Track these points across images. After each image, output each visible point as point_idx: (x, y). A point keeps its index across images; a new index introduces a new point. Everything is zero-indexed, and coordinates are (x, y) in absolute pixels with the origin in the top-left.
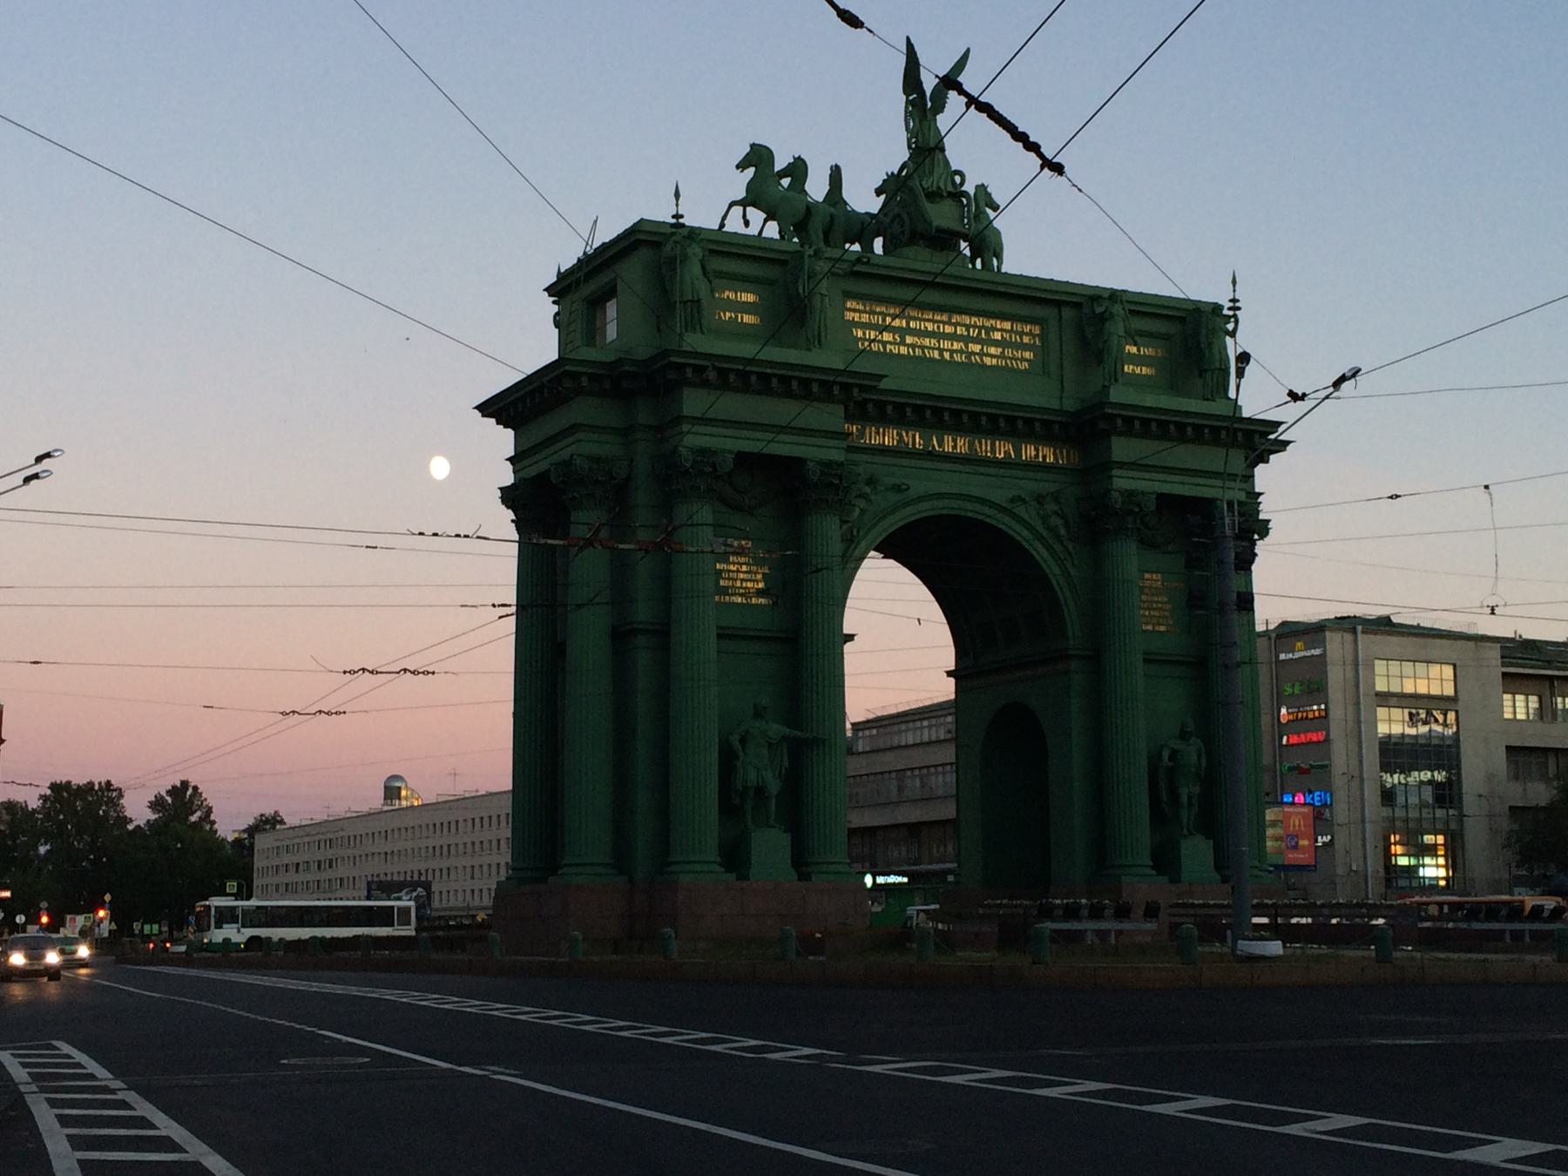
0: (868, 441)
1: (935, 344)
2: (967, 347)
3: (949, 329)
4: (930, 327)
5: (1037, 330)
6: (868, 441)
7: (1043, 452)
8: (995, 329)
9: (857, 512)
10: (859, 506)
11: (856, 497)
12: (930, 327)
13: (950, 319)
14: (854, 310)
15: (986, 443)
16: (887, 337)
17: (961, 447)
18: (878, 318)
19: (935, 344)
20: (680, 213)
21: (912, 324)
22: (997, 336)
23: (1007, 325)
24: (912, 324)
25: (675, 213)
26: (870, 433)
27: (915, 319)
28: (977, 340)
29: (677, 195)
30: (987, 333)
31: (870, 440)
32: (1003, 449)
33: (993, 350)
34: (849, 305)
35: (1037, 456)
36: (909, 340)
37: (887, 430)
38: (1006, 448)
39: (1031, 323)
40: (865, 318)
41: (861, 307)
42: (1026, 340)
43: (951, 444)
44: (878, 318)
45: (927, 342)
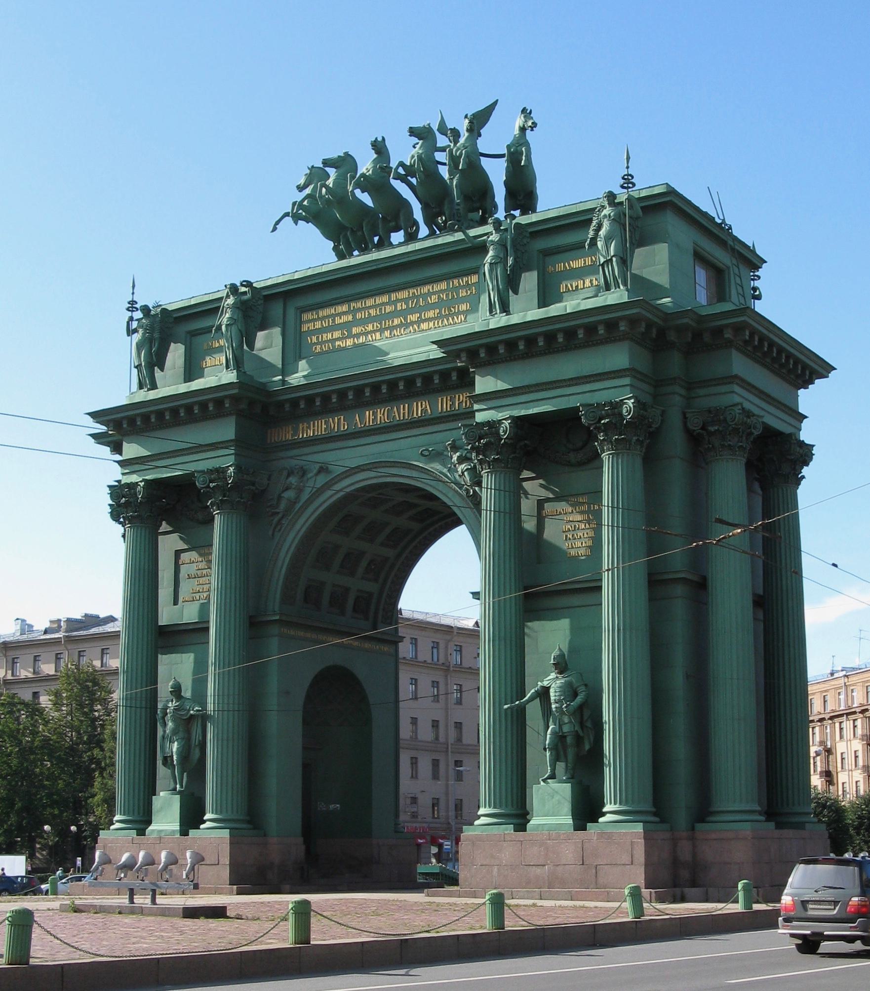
0: (301, 436)
1: (377, 327)
2: (405, 319)
3: (389, 309)
4: (373, 312)
5: (474, 279)
6: (301, 436)
7: (459, 400)
8: (430, 294)
9: (283, 505)
10: (283, 497)
11: (283, 491)
12: (373, 312)
13: (390, 298)
14: (309, 321)
15: (404, 409)
16: (337, 334)
17: (380, 417)
18: (329, 321)
19: (377, 327)
20: (134, 299)
21: (358, 316)
22: (434, 299)
23: (443, 286)
24: (358, 316)
25: (131, 299)
26: (303, 428)
27: (359, 310)
28: (412, 311)
29: (134, 287)
30: (425, 300)
31: (303, 435)
32: (420, 408)
33: (431, 314)
34: (305, 317)
35: (453, 404)
36: (355, 330)
37: (316, 422)
38: (424, 406)
39: (467, 275)
40: (318, 325)
41: (316, 317)
42: (463, 293)
43: (371, 417)
44: (329, 321)
45: (370, 328)
